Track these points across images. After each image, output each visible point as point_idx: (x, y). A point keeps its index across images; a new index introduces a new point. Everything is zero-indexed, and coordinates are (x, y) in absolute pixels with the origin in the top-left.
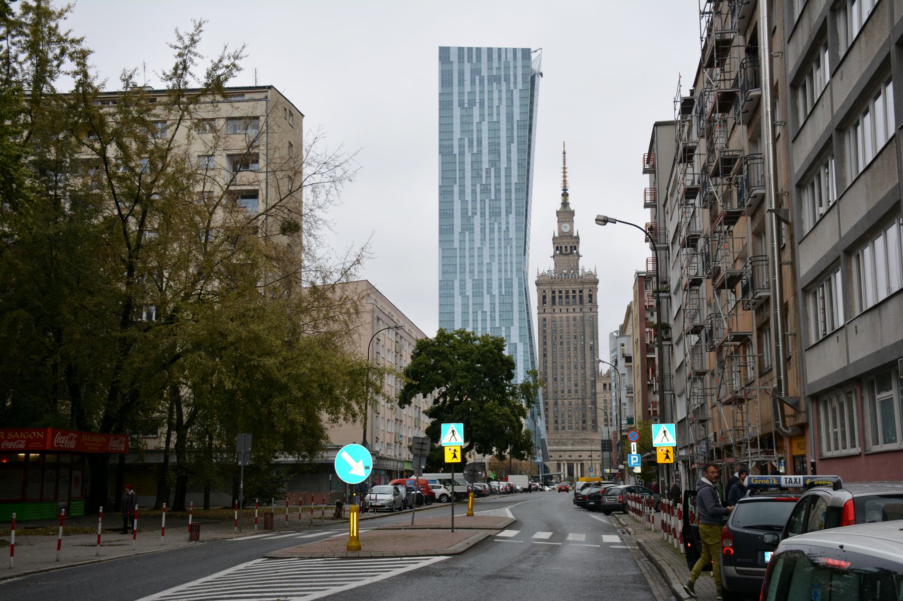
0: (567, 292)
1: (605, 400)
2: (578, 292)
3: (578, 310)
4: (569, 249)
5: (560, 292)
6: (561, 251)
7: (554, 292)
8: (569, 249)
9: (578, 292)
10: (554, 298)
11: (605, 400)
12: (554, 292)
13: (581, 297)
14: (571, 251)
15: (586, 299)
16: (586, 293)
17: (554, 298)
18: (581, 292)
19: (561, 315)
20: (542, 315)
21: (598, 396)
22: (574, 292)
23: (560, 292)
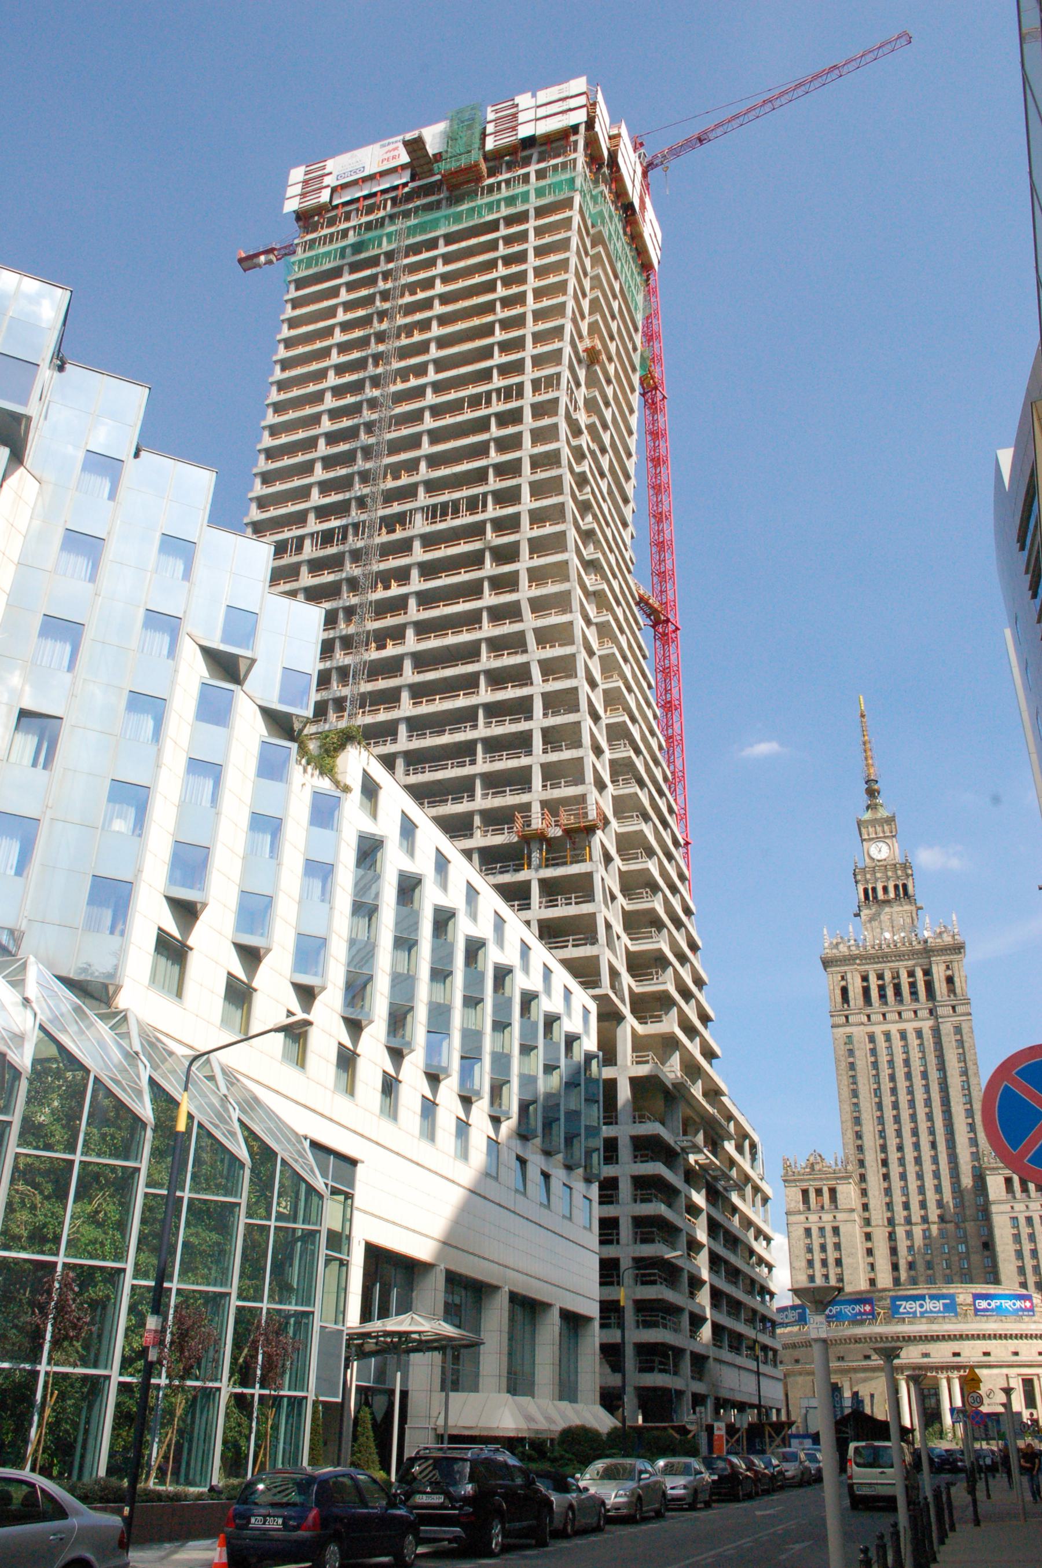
0: (896, 976)
1: (1015, 1219)
2: (919, 974)
3: (924, 1013)
4: (891, 890)
5: (880, 977)
6: (875, 897)
7: (865, 978)
8: (891, 890)
9: (919, 974)
10: (866, 991)
11: (1015, 1219)
12: (865, 978)
13: (929, 986)
14: (897, 895)
15: (940, 987)
16: (939, 973)
17: (866, 991)
18: (927, 972)
19: (886, 1027)
20: (841, 1030)
21: (994, 1208)
22: (911, 974)
23: (880, 977)
